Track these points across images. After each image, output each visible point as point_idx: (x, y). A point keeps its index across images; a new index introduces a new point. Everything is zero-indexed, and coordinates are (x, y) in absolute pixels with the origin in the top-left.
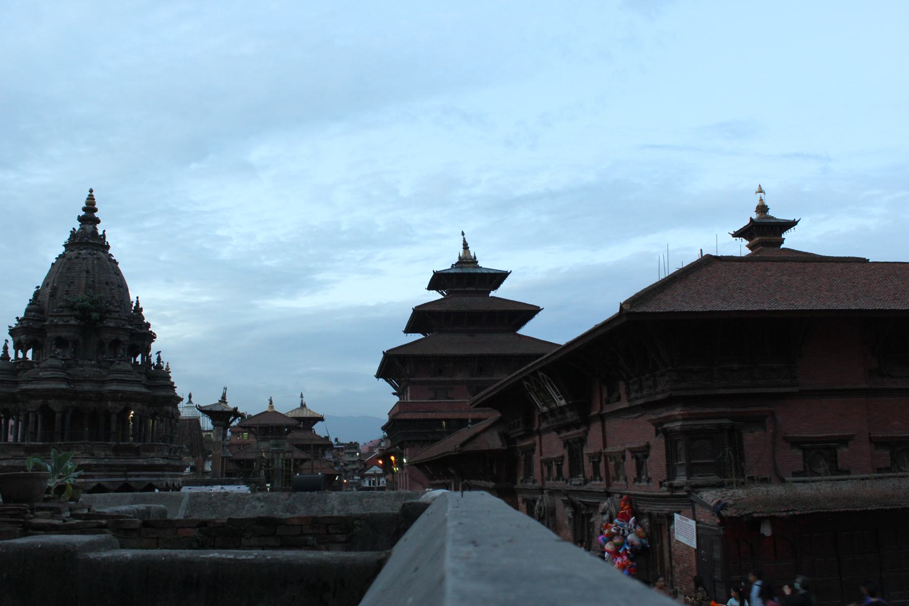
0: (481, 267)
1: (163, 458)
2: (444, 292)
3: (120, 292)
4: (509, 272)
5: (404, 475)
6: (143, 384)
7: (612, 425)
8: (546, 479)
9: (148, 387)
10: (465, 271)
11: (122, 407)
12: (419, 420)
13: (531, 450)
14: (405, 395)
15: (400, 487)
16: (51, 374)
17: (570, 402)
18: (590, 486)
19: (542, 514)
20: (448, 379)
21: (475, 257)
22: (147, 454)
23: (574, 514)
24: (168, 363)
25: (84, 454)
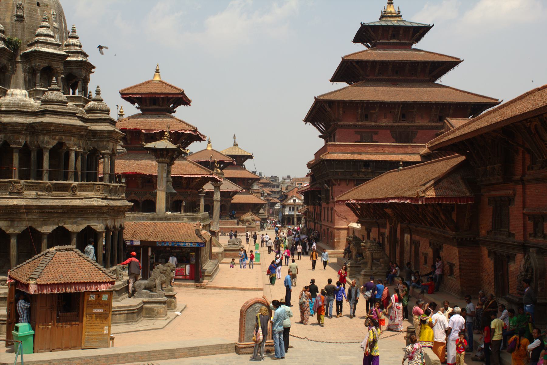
0: (405, 21)
1: (103, 199)
2: (368, 44)
3: (54, 15)
4: (431, 25)
5: (330, 209)
6: (78, 117)
8: (530, 235)
10: (390, 24)
11: (54, 143)
13: (510, 200)
14: (332, 139)
15: (324, 220)
19: (529, 276)
20: (373, 124)
21: (399, 12)
22: (84, 194)
24: (121, 107)
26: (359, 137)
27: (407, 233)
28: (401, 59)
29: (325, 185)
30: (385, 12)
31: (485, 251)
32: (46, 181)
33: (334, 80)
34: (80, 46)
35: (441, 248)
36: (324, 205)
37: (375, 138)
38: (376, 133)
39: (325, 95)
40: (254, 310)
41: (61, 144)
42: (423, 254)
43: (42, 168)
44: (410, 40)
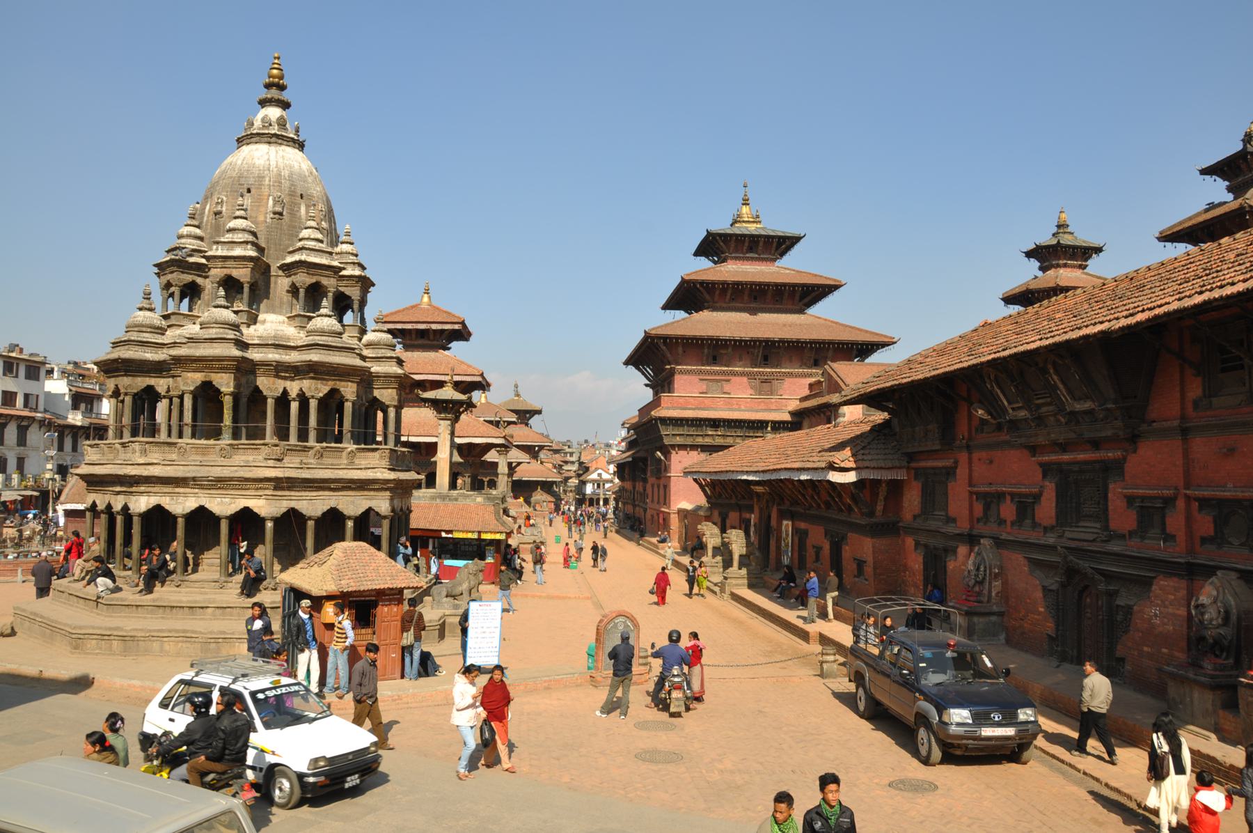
1: (389, 469)
2: (716, 259)
4: (802, 235)
5: (662, 487)
6: (358, 354)
7: (1202, 446)
8: (978, 520)
9: (363, 358)
12: (687, 420)
13: (950, 472)
15: (652, 501)
16: (216, 333)
17: (1110, 406)
18: (1115, 547)
21: (758, 217)
23: (1063, 585)
25: (269, 461)
26: (705, 387)
27: (787, 519)
28: (761, 280)
29: (659, 453)
30: (739, 216)
31: (910, 542)
32: (312, 442)
33: (666, 307)
34: (356, 255)
35: (844, 538)
36: (651, 480)
37: (727, 388)
38: (729, 381)
39: (658, 327)
40: (616, 625)
41: (334, 392)
42: (814, 547)
43: (308, 425)
44: (774, 255)
